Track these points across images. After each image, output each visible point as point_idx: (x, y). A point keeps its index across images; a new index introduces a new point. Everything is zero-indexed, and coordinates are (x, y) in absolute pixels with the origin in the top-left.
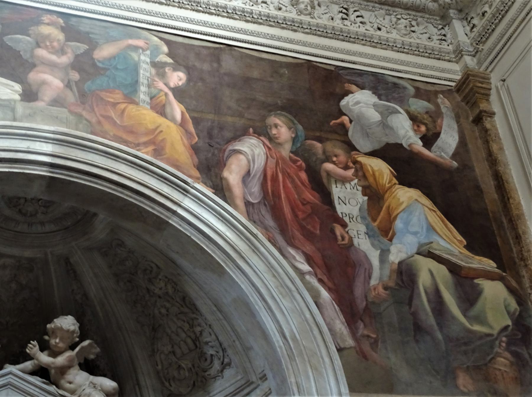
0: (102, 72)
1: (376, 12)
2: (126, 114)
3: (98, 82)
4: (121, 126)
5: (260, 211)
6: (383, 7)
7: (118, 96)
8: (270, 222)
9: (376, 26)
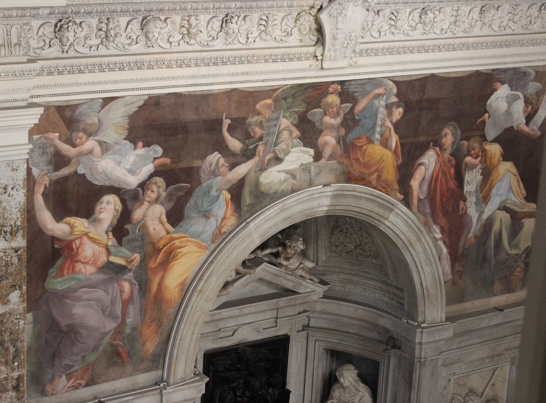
2: (366, 152)
8: (428, 210)
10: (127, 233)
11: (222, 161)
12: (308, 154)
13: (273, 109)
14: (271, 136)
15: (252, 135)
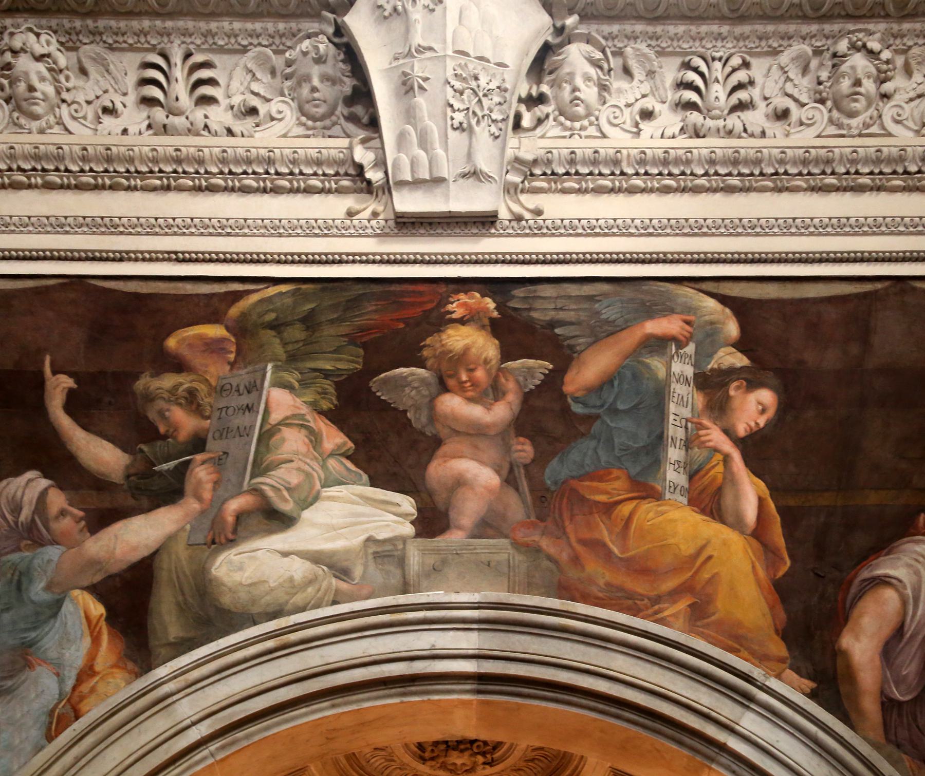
0: (582, 429)
3: (575, 455)
4: (621, 559)
5: (915, 720)
7: (617, 484)
11: (57, 500)
12: (394, 509)
13: (232, 357)
14: (237, 439)
15: (162, 429)
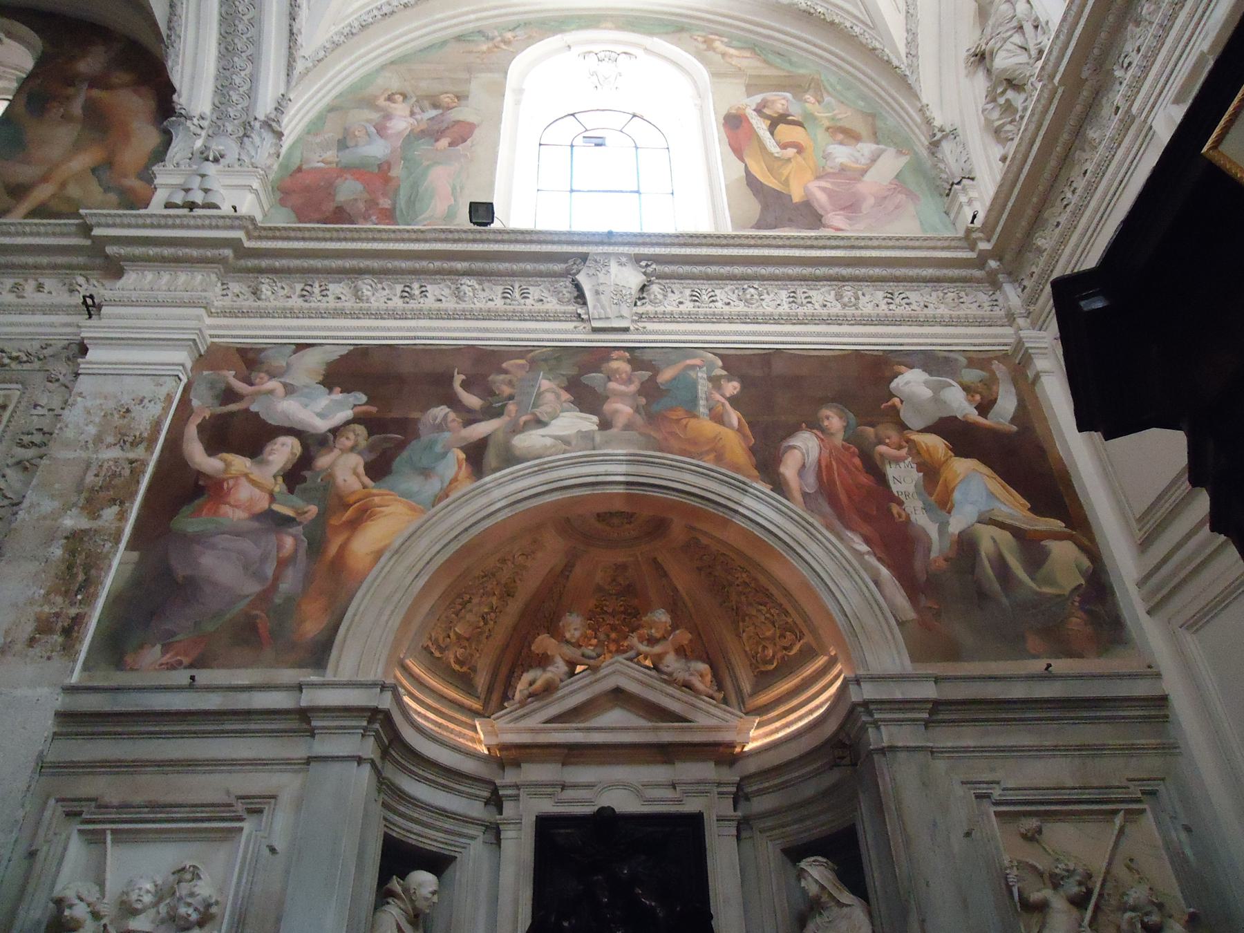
1: (922, 291)
2: (688, 428)
6: (928, 284)
8: (827, 509)
9: (922, 304)
10: (304, 479)
11: (452, 415)
13: (527, 369)
